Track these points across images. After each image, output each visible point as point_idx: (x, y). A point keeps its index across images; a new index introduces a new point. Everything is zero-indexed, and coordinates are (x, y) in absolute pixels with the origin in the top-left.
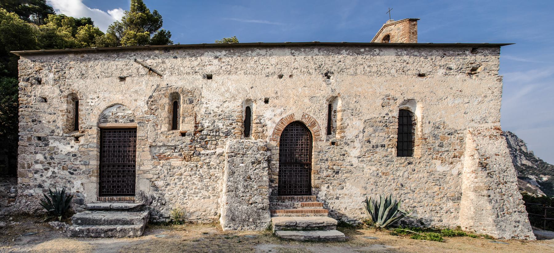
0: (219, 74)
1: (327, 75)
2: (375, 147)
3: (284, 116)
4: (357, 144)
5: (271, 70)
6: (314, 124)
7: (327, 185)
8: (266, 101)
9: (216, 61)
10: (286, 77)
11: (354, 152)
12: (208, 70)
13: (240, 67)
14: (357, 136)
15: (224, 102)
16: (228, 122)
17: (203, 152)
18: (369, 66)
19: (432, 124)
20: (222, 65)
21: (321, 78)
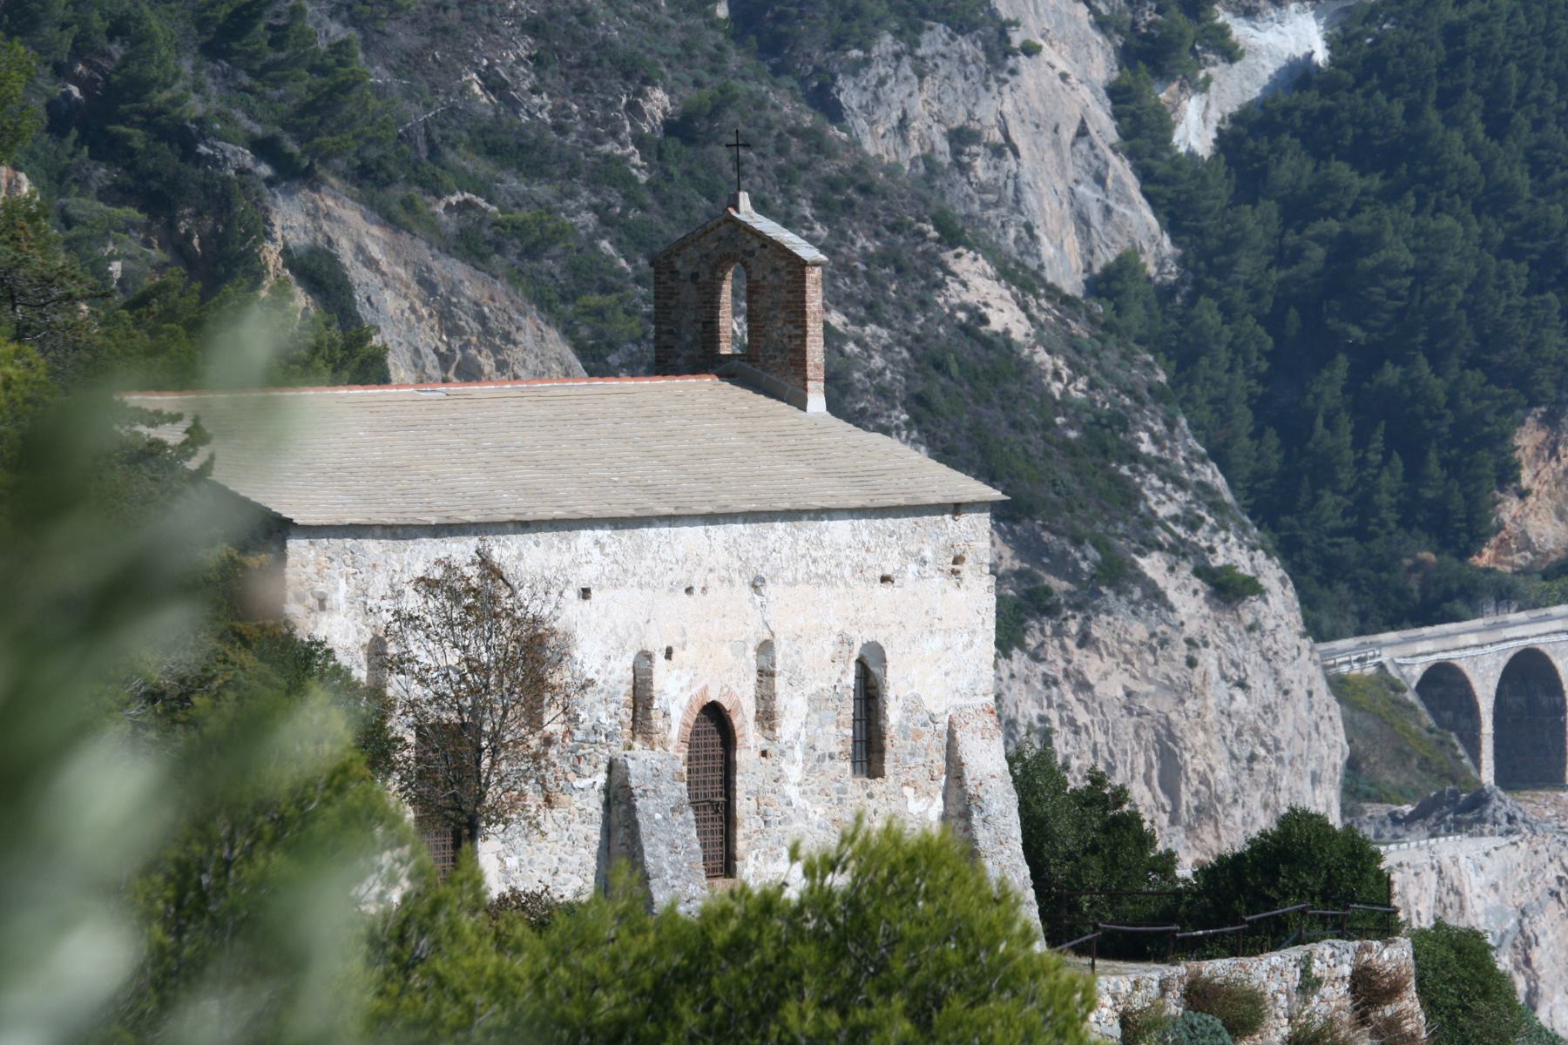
0: (601, 588)
1: (757, 585)
2: (821, 759)
3: (695, 691)
4: (799, 755)
5: (679, 574)
6: (738, 704)
7: (754, 853)
8: (669, 654)
9: (596, 551)
10: (697, 591)
11: (794, 772)
12: (586, 576)
13: (631, 568)
14: (798, 736)
15: (608, 658)
16: (612, 707)
17: (578, 783)
18: (814, 561)
19: (900, 703)
20: (607, 560)
21: (747, 592)
